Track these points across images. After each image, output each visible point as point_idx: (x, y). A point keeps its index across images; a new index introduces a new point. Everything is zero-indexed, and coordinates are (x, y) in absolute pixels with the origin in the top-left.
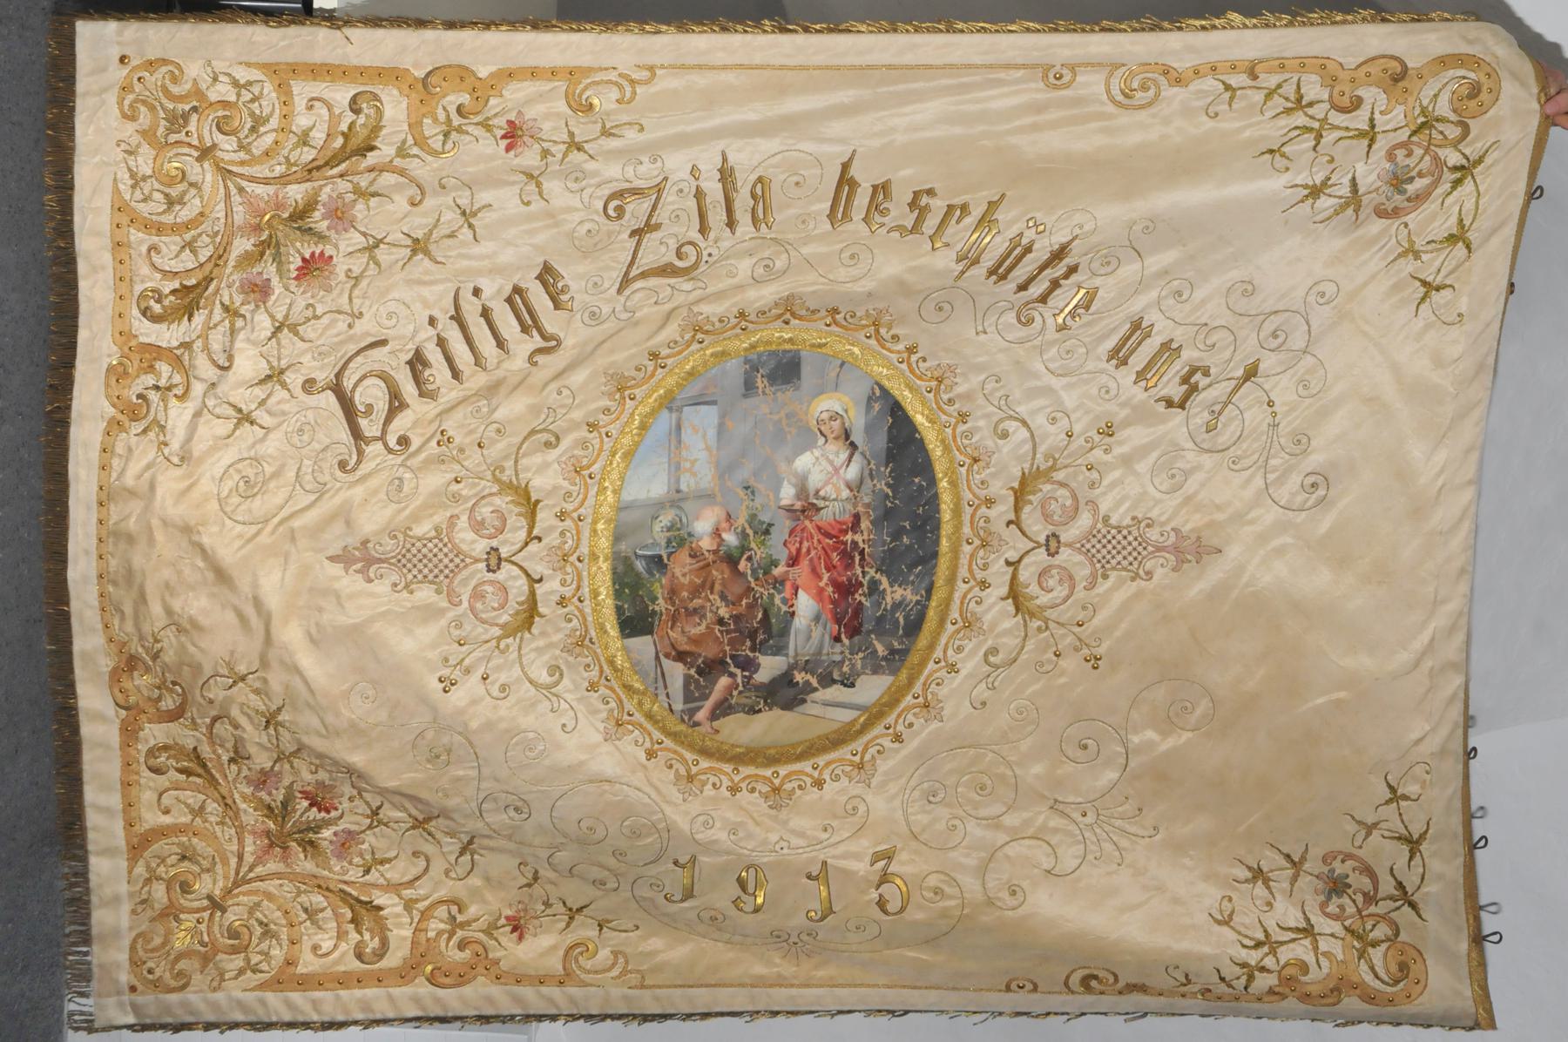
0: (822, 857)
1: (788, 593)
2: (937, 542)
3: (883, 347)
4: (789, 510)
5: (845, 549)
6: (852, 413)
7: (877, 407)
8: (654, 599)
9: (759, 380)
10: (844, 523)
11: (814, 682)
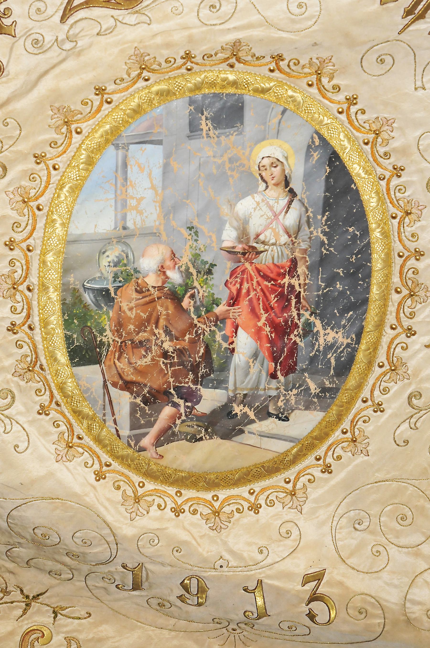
0: (260, 577)
1: (228, 329)
2: (368, 289)
3: (324, 97)
4: (231, 252)
5: (283, 291)
6: (292, 161)
7: (316, 156)
8: (102, 331)
9: (203, 122)
10: (283, 268)
11: (252, 415)
